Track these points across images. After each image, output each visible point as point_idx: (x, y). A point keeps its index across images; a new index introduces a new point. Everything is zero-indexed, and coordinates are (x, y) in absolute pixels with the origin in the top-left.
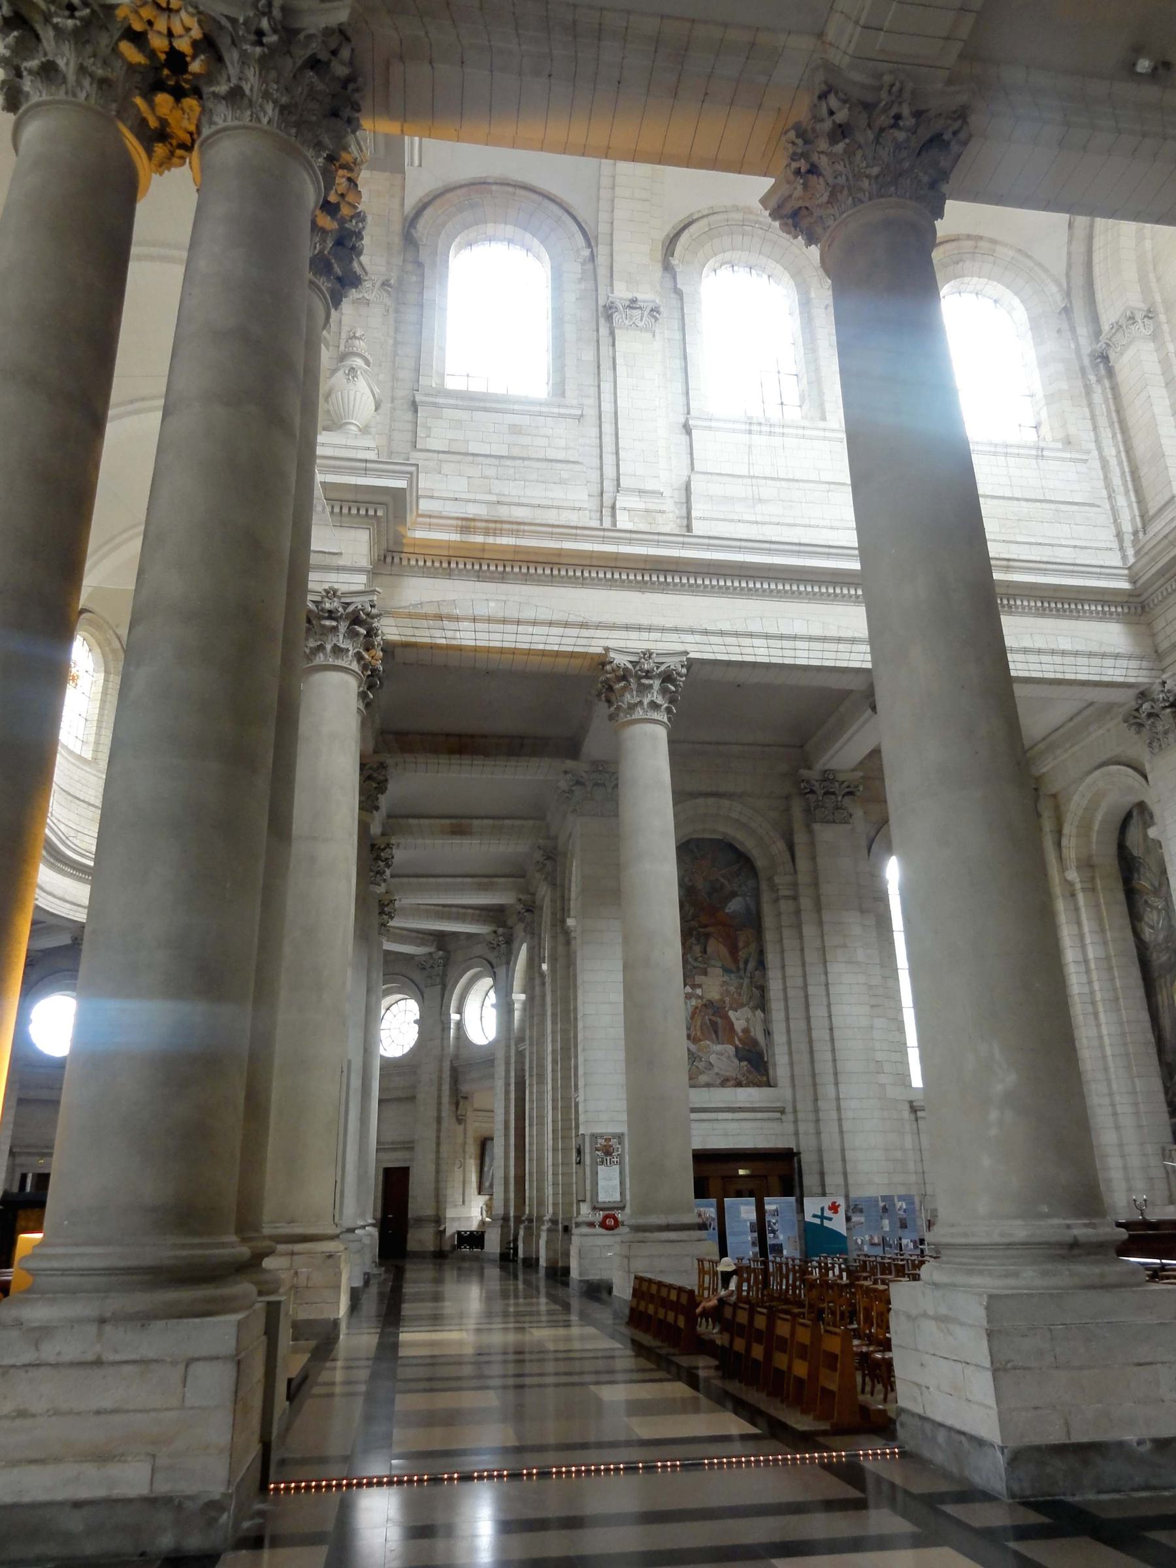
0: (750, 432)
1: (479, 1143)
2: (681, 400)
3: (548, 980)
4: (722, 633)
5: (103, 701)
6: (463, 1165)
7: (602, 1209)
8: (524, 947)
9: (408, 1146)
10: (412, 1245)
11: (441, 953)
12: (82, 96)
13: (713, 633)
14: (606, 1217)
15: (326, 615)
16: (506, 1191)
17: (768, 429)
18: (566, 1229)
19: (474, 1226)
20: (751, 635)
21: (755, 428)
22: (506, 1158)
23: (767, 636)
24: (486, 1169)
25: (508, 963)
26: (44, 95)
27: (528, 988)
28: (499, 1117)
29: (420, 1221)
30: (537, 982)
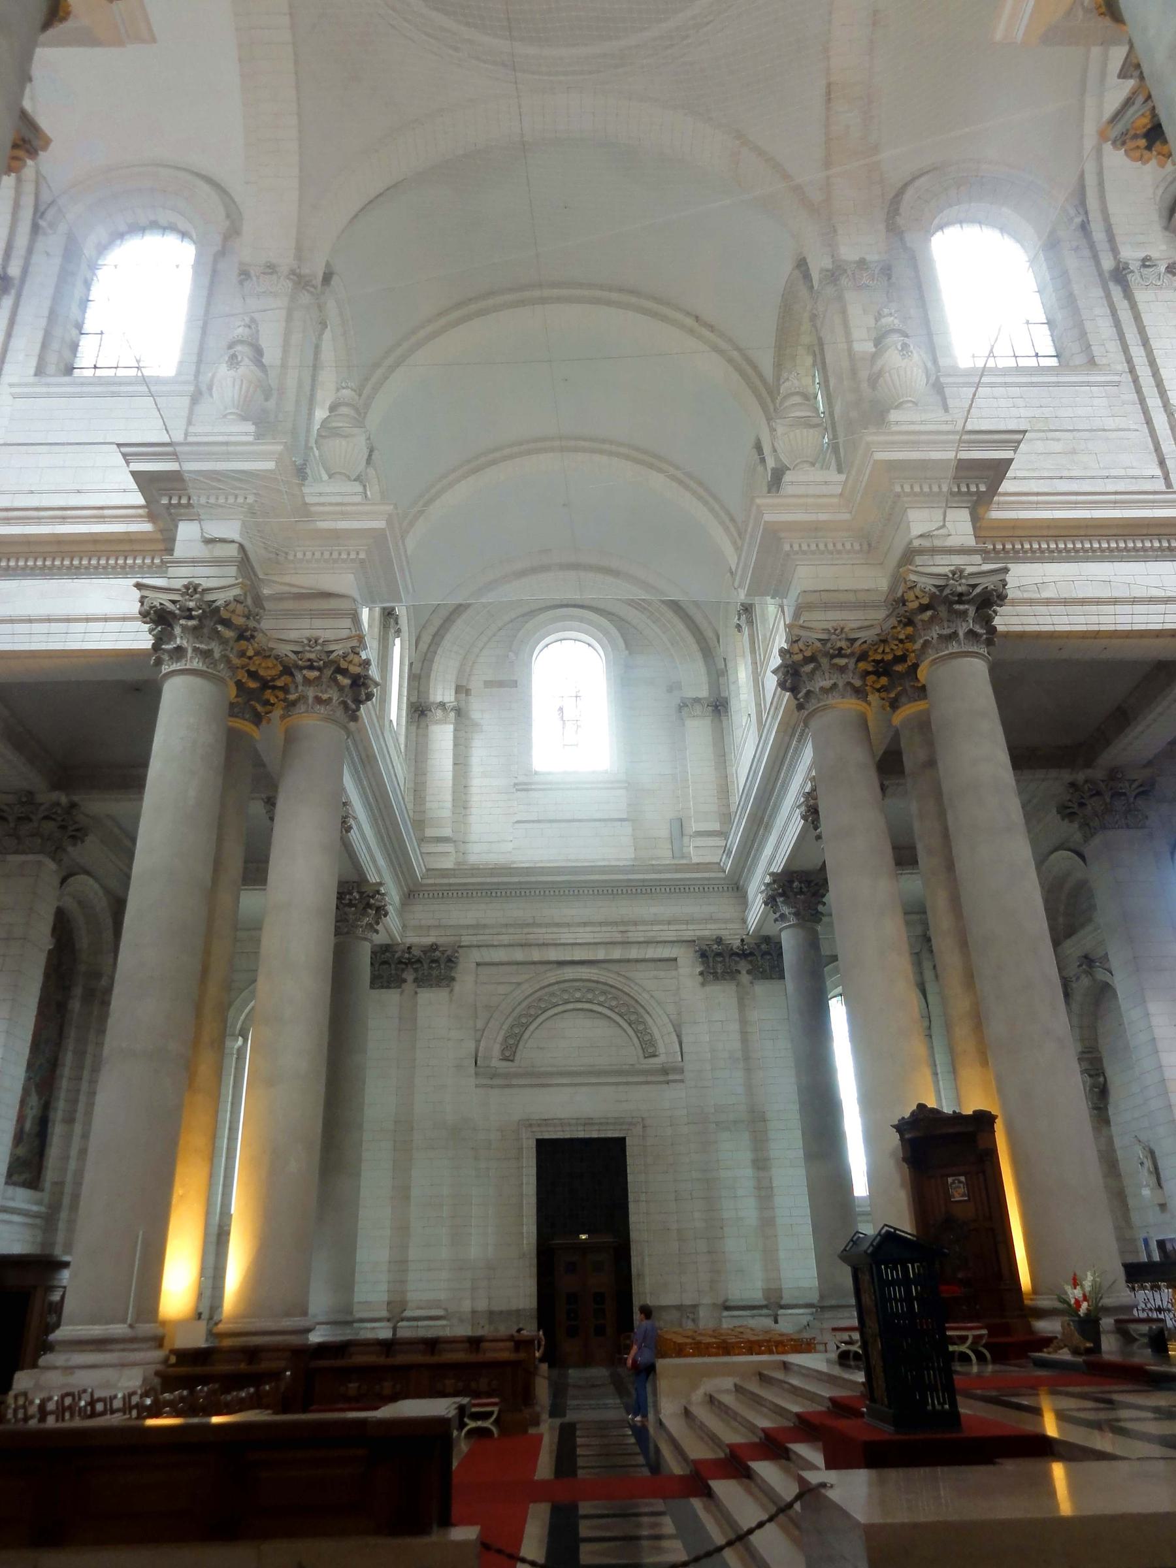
15: (956, 598)
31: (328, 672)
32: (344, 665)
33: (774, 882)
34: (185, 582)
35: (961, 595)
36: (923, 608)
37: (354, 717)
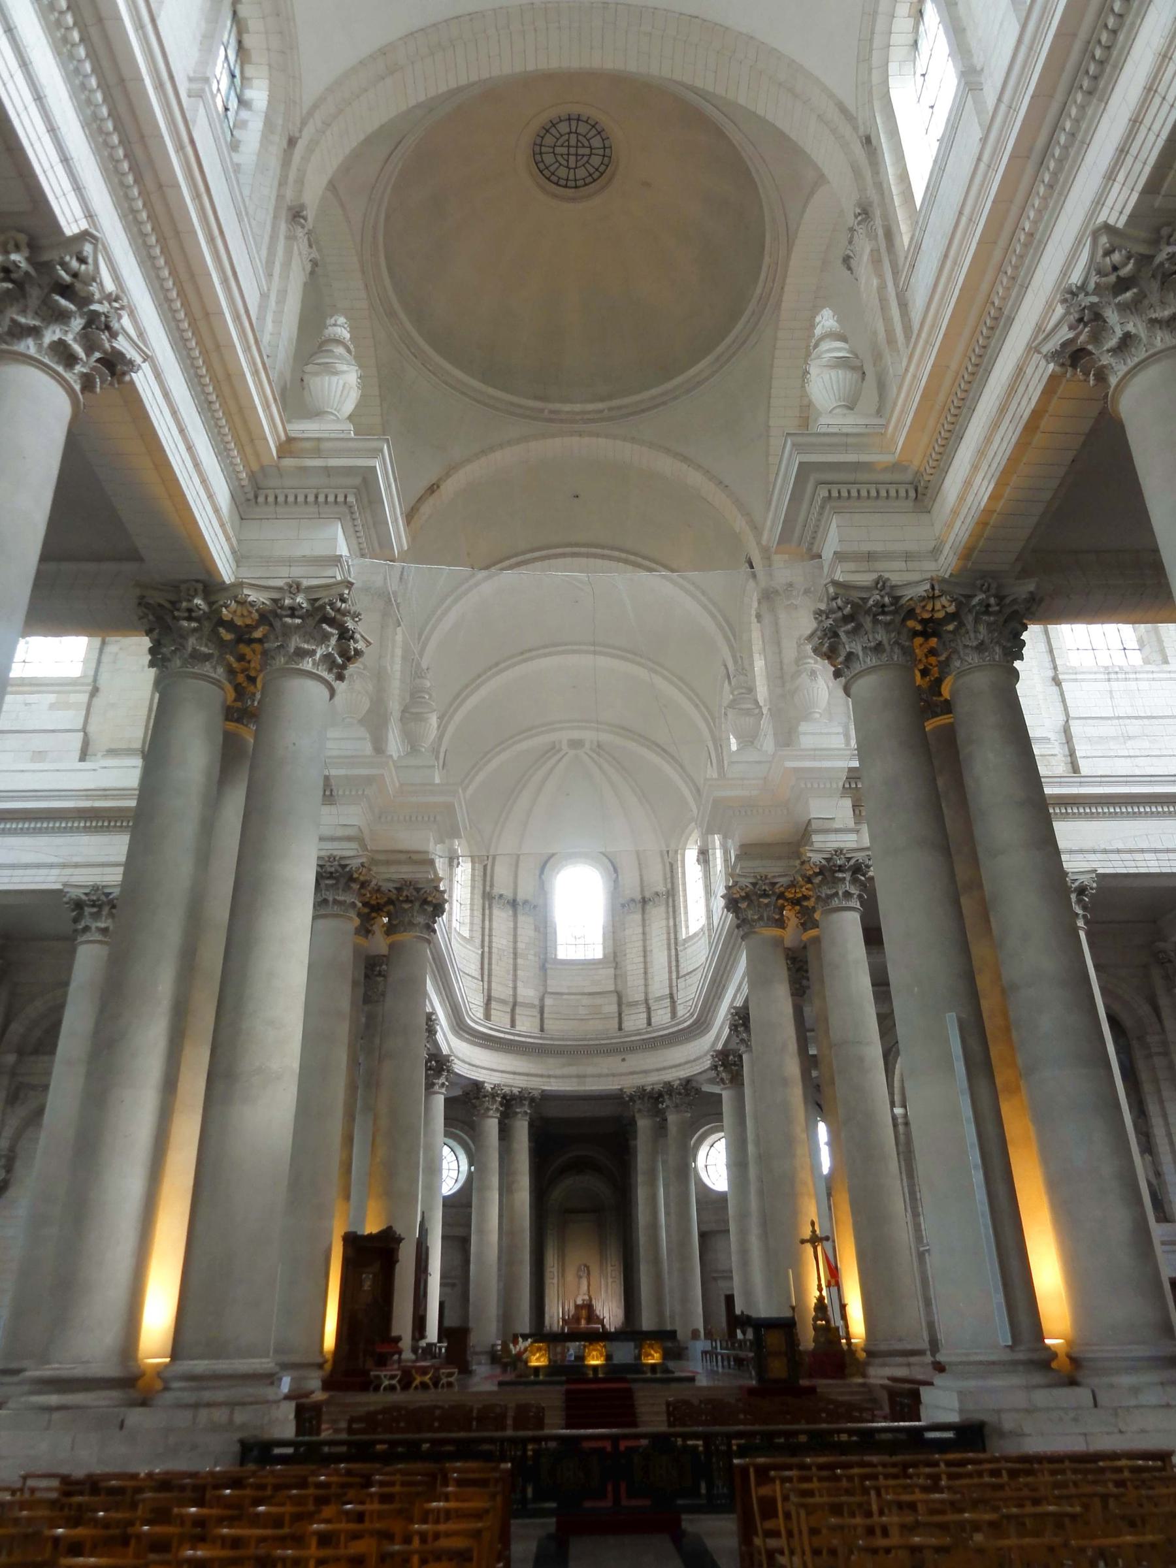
0: (1109, 680)
2: (1047, 658)
4: (1118, 851)
5: (473, 887)
12: (895, 658)
13: (1112, 852)
17: (1124, 676)
20: (1142, 851)
21: (1113, 676)
23: (1156, 851)
26: (874, 660)
31: (417, 905)
32: (430, 899)
33: (737, 1014)
34: (328, 853)
35: (840, 866)
36: (816, 874)
37: (434, 931)
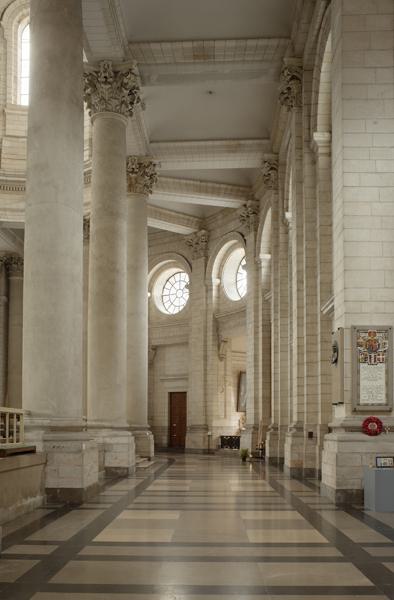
1: (236, 375)
3: (293, 225)
6: (224, 390)
7: (363, 412)
8: (269, 213)
9: (184, 378)
10: (188, 444)
11: (203, 231)
14: (369, 421)
16: (256, 408)
18: (311, 435)
19: (233, 433)
22: (256, 383)
24: (242, 393)
25: (256, 230)
27: (274, 249)
28: (251, 353)
29: (194, 428)
30: (282, 230)
